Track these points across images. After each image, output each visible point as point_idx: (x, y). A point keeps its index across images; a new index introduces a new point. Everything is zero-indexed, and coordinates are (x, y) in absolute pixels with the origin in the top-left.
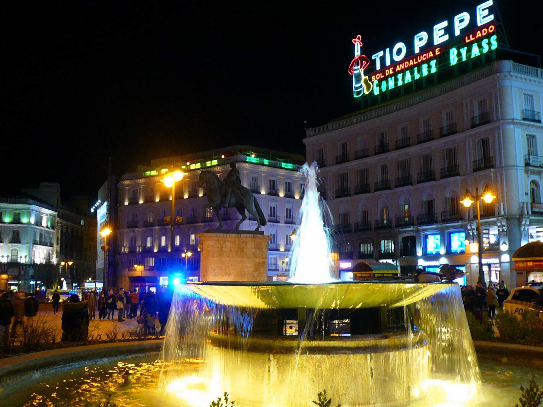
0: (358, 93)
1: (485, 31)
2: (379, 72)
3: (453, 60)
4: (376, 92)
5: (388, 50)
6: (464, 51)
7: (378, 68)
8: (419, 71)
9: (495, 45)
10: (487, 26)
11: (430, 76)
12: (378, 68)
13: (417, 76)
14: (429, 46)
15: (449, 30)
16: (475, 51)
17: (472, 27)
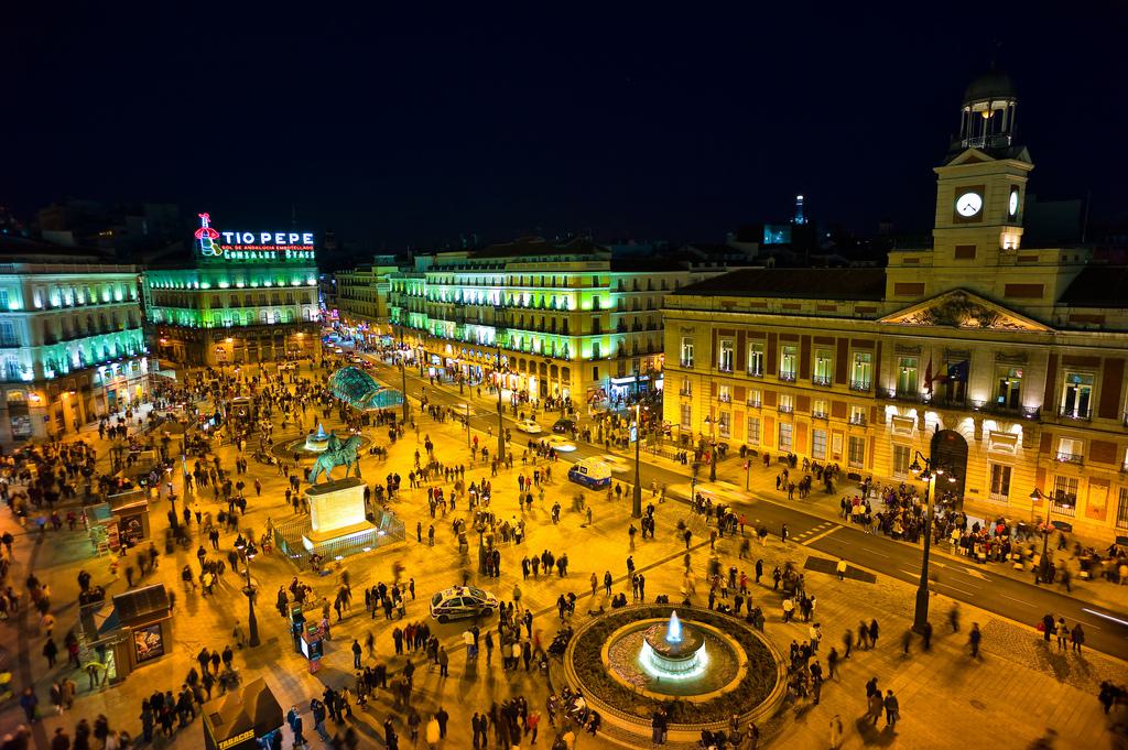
0: (208, 253)
1: (308, 248)
2: (229, 245)
3: (288, 255)
4: (227, 257)
5: (238, 234)
6: (295, 253)
7: (229, 241)
8: (263, 254)
9: (313, 256)
10: (309, 245)
11: (270, 260)
12: (229, 241)
13: (261, 257)
14: (272, 243)
15: (286, 238)
16: (301, 255)
17: (300, 244)
